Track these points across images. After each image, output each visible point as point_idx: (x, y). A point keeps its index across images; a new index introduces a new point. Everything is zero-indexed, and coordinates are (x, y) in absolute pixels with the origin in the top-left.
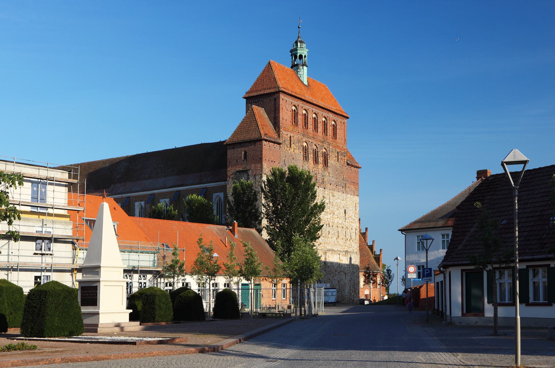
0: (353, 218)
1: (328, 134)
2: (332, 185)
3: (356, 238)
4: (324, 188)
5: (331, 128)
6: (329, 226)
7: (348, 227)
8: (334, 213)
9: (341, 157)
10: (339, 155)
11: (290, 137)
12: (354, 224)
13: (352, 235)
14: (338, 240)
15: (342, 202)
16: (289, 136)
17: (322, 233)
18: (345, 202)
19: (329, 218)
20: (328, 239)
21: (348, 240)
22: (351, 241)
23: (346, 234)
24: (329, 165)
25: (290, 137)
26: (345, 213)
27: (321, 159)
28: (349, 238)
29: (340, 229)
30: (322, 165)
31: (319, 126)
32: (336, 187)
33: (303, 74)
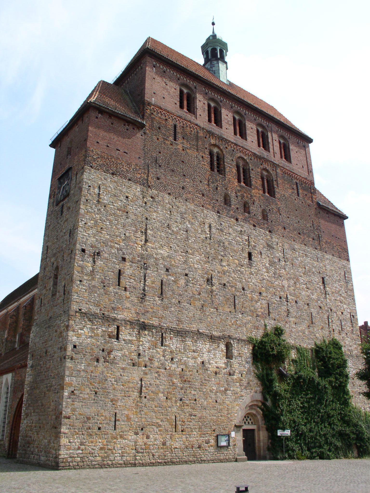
0: (343, 295)
1: (271, 150)
2: (287, 230)
3: (352, 330)
4: (270, 231)
5: (277, 144)
6: (287, 302)
7: (334, 309)
8: (298, 279)
9: (305, 193)
10: (299, 188)
11: (175, 126)
12: (345, 306)
13: (343, 323)
14: (311, 329)
15: (315, 263)
16: (171, 123)
17: (271, 311)
18: (321, 265)
19: (286, 286)
20: (287, 326)
21: (336, 332)
22: (343, 335)
23: (330, 320)
24: (277, 195)
25: (175, 126)
26: (323, 283)
27: (256, 181)
28: (338, 328)
29: (314, 311)
30: (261, 192)
31: (248, 132)
32: (298, 236)
33: (218, 69)
